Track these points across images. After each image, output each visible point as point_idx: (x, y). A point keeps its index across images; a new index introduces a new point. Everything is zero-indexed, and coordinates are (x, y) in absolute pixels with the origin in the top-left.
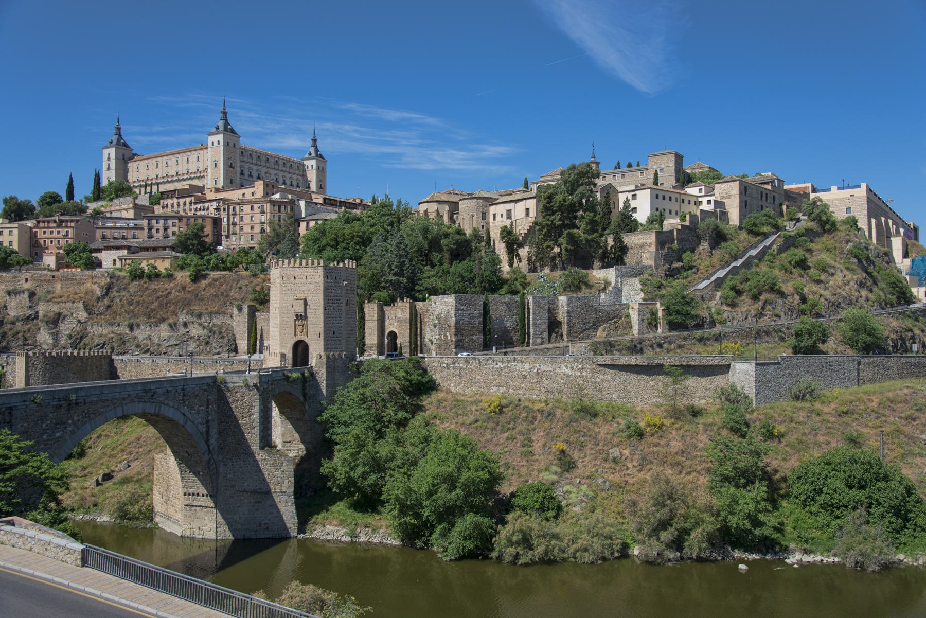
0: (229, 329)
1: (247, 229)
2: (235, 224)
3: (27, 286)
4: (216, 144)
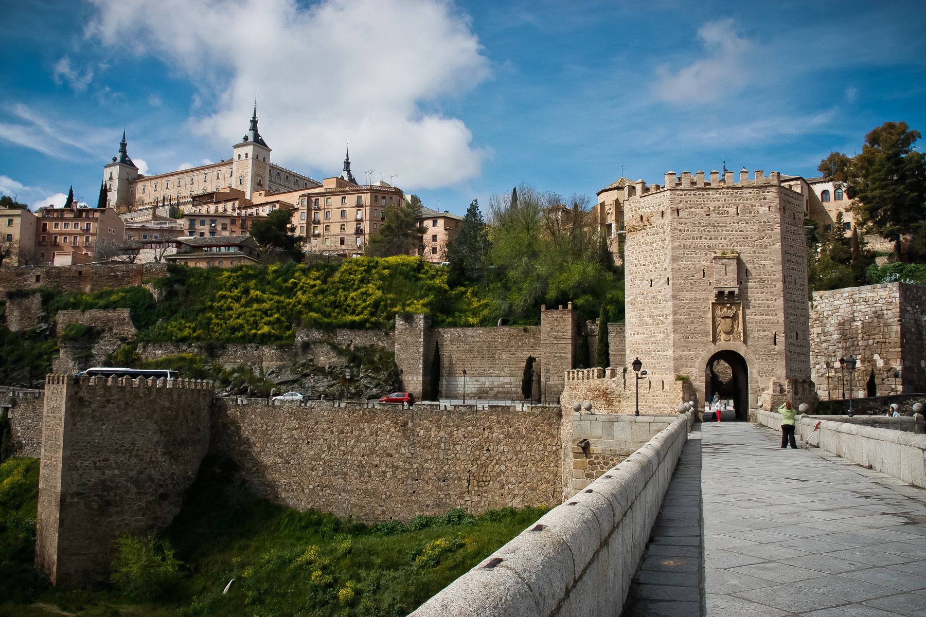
0: (388, 357)
1: (335, 229)
2: (317, 223)
3: (37, 286)
4: (243, 157)
